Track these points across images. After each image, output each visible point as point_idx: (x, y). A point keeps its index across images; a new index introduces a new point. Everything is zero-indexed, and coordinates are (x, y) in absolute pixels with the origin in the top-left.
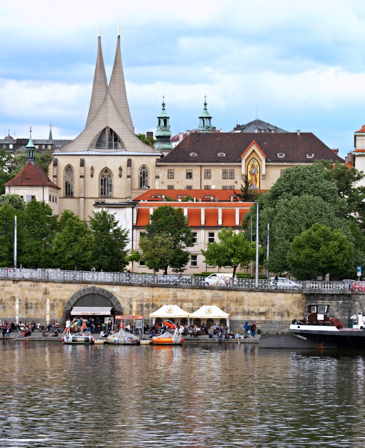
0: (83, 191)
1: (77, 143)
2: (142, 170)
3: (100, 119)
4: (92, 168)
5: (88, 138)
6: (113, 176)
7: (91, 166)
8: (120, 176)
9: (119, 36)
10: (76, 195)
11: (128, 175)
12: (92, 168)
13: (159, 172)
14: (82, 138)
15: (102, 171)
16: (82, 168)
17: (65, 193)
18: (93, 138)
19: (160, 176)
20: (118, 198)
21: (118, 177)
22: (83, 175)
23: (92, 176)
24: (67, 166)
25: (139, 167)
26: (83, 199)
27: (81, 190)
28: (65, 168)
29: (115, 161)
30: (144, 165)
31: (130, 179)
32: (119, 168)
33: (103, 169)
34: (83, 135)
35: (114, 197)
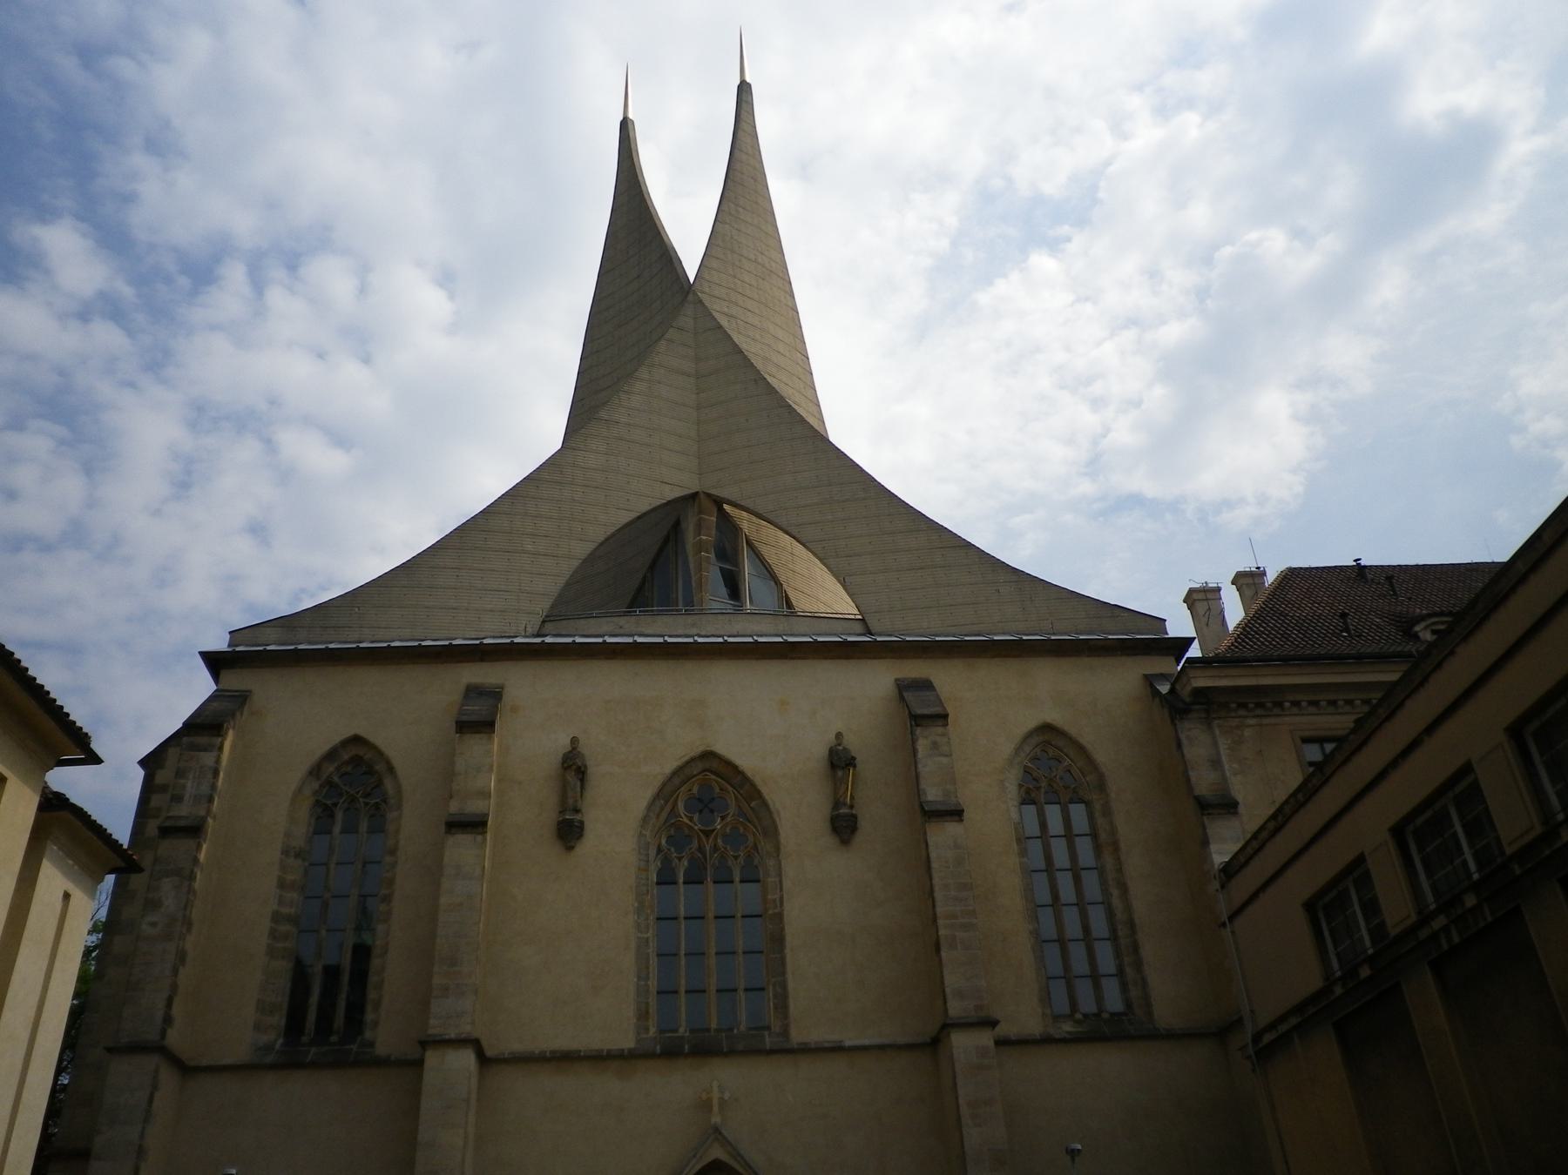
4: (574, 767)
6: (772, 832)
7: (562, 742)
8: (843, 826)
10: (386, 1035)
11: (932, 794)
12: (574, 767)
13: (1216, 763)
15: (665, 793)
17: (279, 1020)
18: (583, 549)
19: (1240, 789)
20: (838, 1049)
23: (569, 832)
24: (331, 755)
25: (1007, 749)
26: (465, 1060)
28: (315, 771)
30: (1046, 728)
31: (952, 828)
33: (681, 774)
35: (797, 1036)
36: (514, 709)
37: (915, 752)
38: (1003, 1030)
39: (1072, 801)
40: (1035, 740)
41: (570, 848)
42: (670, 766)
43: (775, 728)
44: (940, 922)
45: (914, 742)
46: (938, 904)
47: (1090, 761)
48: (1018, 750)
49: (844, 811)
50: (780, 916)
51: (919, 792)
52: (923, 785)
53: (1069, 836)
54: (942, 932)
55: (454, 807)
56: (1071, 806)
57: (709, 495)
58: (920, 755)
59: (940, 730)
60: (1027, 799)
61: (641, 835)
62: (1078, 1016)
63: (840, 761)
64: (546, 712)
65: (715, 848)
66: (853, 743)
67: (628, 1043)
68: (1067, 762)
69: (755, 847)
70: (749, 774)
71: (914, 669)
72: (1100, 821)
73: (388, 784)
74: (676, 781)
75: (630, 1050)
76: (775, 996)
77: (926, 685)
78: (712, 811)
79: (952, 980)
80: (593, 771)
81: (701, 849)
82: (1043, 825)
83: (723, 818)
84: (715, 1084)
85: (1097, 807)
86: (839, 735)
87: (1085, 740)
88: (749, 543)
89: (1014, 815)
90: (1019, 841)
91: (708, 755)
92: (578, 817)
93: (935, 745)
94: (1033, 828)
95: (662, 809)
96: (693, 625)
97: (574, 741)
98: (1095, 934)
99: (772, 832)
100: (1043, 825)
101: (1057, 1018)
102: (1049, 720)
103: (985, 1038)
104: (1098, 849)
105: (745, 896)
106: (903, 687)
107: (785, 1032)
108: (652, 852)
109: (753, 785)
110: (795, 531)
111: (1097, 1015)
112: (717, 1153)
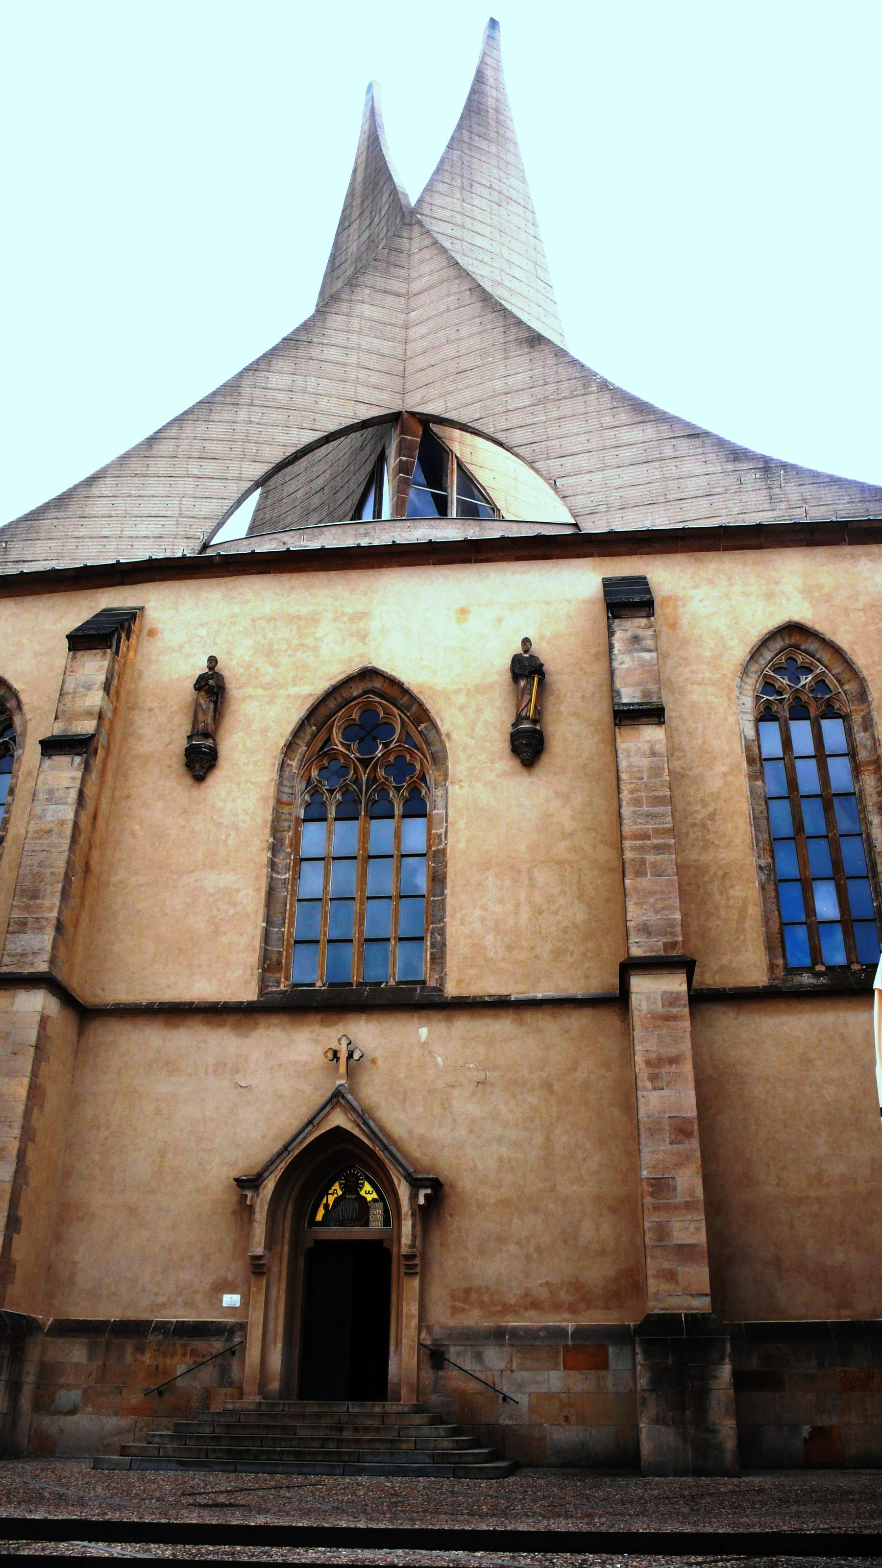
0: (51, 904)
1: (100, 507)
2: (768, 686)
3: (334, 354)
4: (212, 687)
5: (210, 468)
7: (202, 667)
8: (528, 745)
9: (493, 24)
12: (212, 687)
14: (161, 466)
16: (94, 667)
21: (506, 763)
22: (87, 727)
23: (200, 760)
25: (740, 652)
27: (35, 894)
29: (463, 611)
31: (652, 734)
32: (516, 661)
33: (337, 695)
34: (166, 447)
35: (452, 990)
36: (152, 633)
37: (611, 647)
38: (711, 977)
39: (824, 716)
40: (778, 644)
41: (199, 778)
42: (321, 686)
43: (446, 636)
44: (627, 844)
45: (611, 634)
46: (626, 822)
47: (848, 664)
48: (755, 654)
49: (526, 725)
50: (443, 852)
51: (614, 693)
52: (618, 684)
53: (821, 756)
54: (629, 855)
55: (57, 729)
56: (826, 724)
57: (413, 414)
58: (616, 651)
59: (643, 622)
60: (765, 715)
61: (282, 766)
62: (820, 968)
63: (527, 669)
64: (183, 630)
65: (372, 780)
66: (542, 651)
67: (249, 994)
68: (820, 669)
69: (423, 778)
70: (415, 691)
71: (625, 567)
72: (861, 736)
73: (17, 721)
74: (332, 704)
75: (250, 1003)
76: (433, 946)
77: (641, 583)
78: (375, 739)
79: (635, 914)
80: (234, 691)
81: (357, 781)
82: (787, 743)
83: (386, 745)
84: (344, 1042)
85: (857, 718)
86: (526, 642)
87: (842, 640)
88: (460, 466)
89: (750, 733)
90: (750, 761)
91: (368, 673)
92: (209, 743)
93: (636, 639)
94: (772, 745)
95: (314, 736)
96: (366, 535)
97: (213, 661)
98: (849, 870)
99: (439, 759)
100: (787, 743)
101: (790, 971)
102: (796, 618)
103: (677, 984)
104: (856, 771)
105: (415, 834)
106: (609, 585)
107: (440, 989)
108: (300, 786)
109: (421, 705)
110: (500, 436)
111: (847, 968)
112: (338, 1119)
